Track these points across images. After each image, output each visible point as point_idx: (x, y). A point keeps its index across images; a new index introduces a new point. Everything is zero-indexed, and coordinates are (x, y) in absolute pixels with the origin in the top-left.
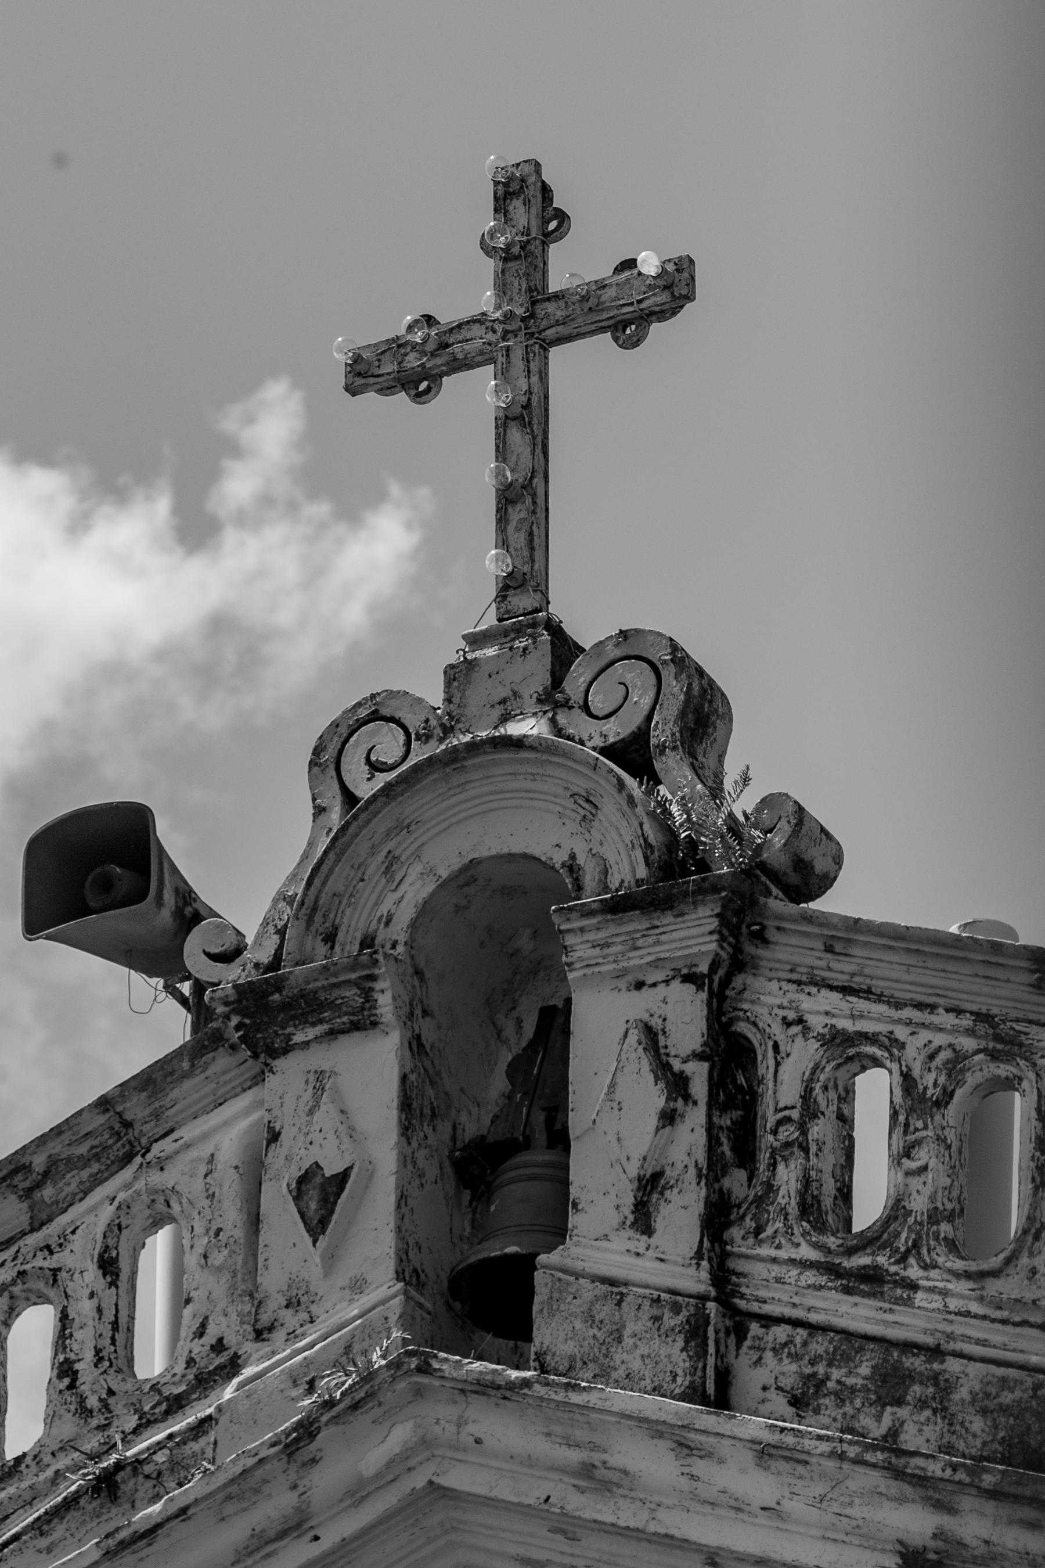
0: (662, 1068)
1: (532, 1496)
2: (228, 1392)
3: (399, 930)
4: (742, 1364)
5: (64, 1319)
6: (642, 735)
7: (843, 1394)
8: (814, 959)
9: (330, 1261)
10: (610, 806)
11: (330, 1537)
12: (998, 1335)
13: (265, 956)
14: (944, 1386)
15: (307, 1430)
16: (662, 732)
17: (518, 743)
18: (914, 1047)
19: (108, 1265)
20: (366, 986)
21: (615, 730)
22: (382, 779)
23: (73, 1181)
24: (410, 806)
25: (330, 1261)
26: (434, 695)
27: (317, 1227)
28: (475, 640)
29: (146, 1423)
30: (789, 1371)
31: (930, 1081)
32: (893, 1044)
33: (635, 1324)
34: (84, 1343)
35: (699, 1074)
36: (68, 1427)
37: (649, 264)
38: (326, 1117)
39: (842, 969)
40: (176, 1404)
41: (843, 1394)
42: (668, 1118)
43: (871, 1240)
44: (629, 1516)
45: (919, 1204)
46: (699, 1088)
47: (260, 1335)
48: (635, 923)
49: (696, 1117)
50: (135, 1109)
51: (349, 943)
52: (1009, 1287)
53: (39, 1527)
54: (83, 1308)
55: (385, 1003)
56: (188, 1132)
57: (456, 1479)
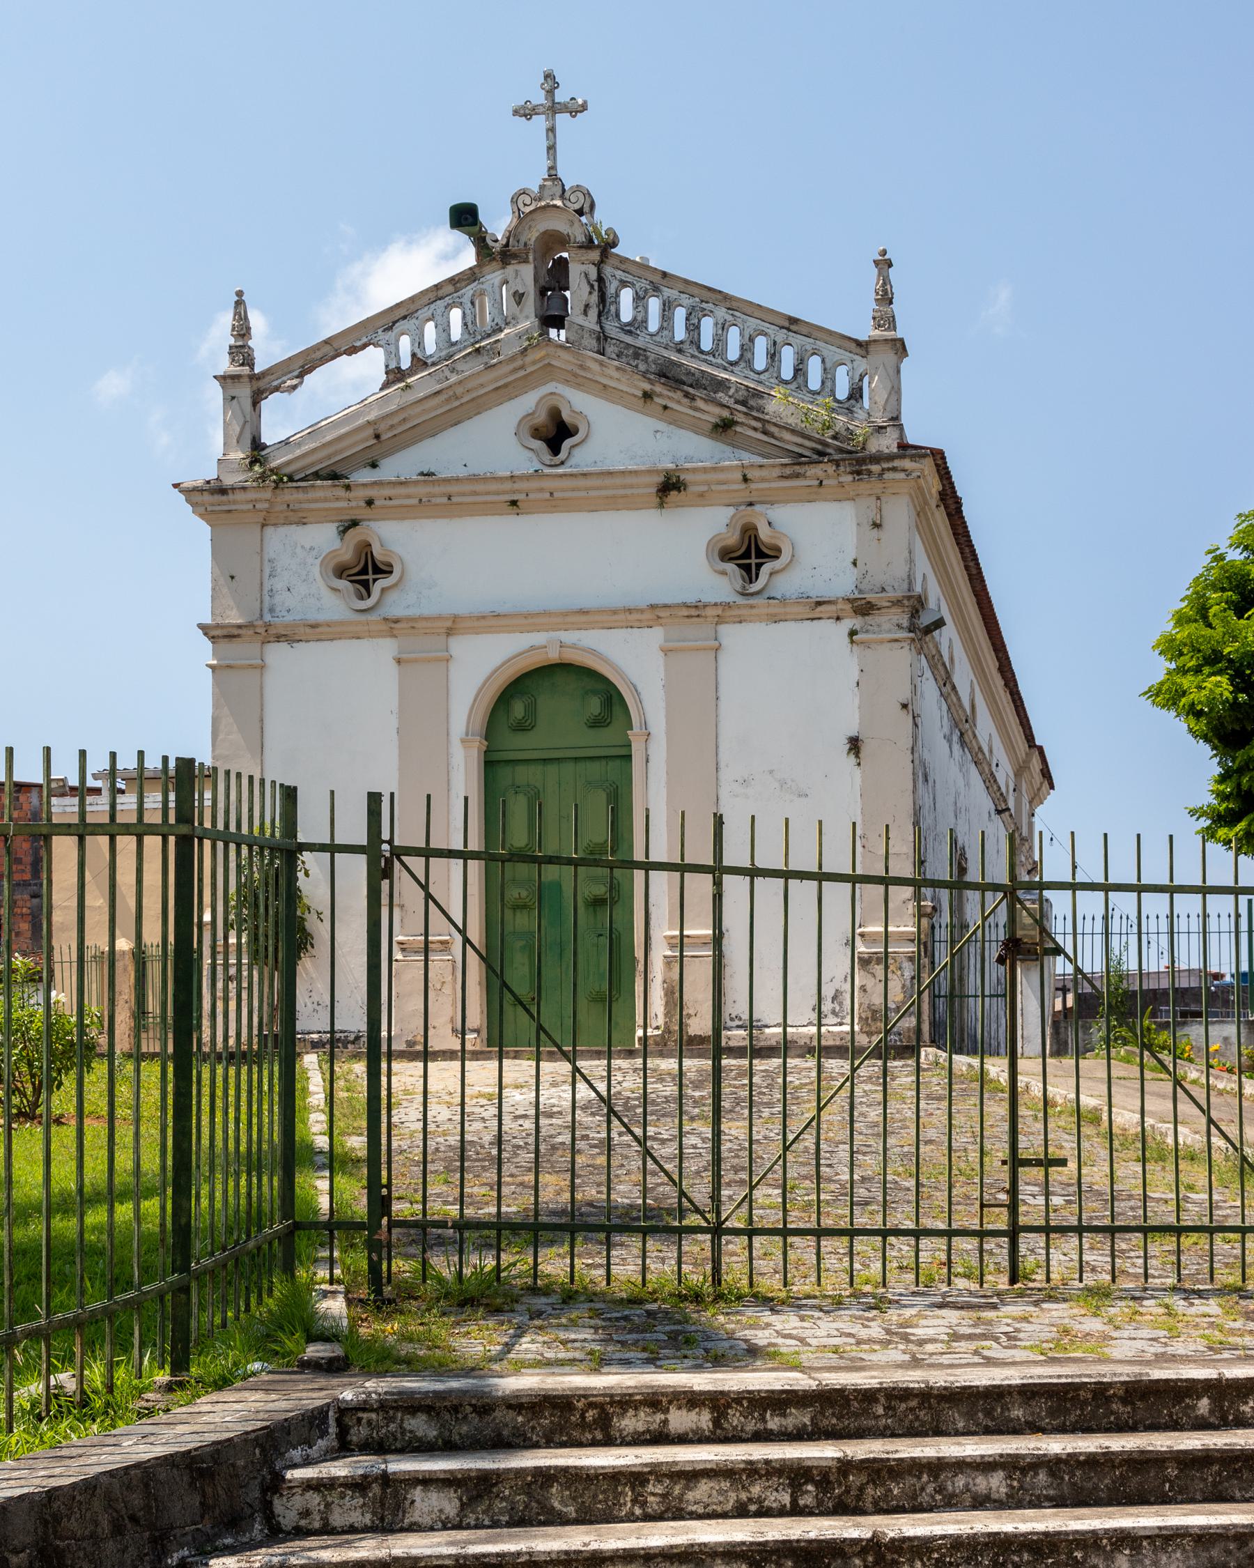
0: (589, 282)
1: (569, 368)
2: (502, 336)
3: (532, 242)
4: (607, 346)
5: (464, 314)
6: (582, 208)
7: (627, 356)
8: (617, 263)
9: (521, 311)
10: (577, 224)
11: (529, 370)
12: (657, 348)
13: (504, 242)
14: (647, 358)
15: (526, 349)
16: (586, 209)
17: (555, 206)
18: (638, 285)
19: (473, 303)
20: (527, 254)
21: (577, 206)
22: (527, 210)
23: (464, 283)
24: (534, 216)
25: (521, 311)
26: (536, 189)
27: (518, 303)
28: (545, 180)
29: (483, 339)
30: (616, 350)
31: (641, 294)
32: (633, 285)
33: (587, 335)
34: (469, 319)
35: (596, 284)
36: (466, 336)
37: (580, 101)
38: (519, 279)
39: (623, 267)
40: (489, 336)
41: (627, 356)
42: (590, 293)
43: (629, 324)
44: (589, 376)
45: (639, 318)
46: (596, 287)
47: (507, 324)
48: (583, 251)
49: (596, 294)
50: (476, 271)
51: (521, 246)
52: (658, 339)
53: (464, 357)
54: (468, 312)
55: (531, 258)
56: (488, 277)
57: (553, 363)
